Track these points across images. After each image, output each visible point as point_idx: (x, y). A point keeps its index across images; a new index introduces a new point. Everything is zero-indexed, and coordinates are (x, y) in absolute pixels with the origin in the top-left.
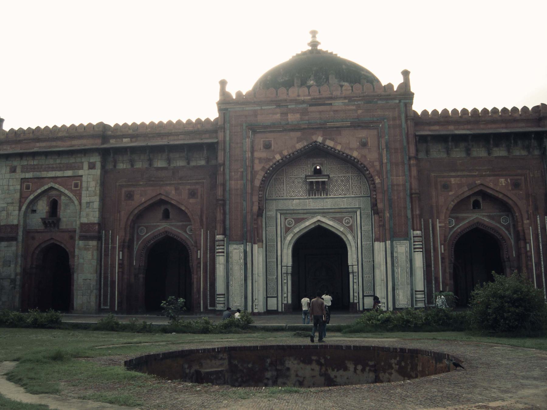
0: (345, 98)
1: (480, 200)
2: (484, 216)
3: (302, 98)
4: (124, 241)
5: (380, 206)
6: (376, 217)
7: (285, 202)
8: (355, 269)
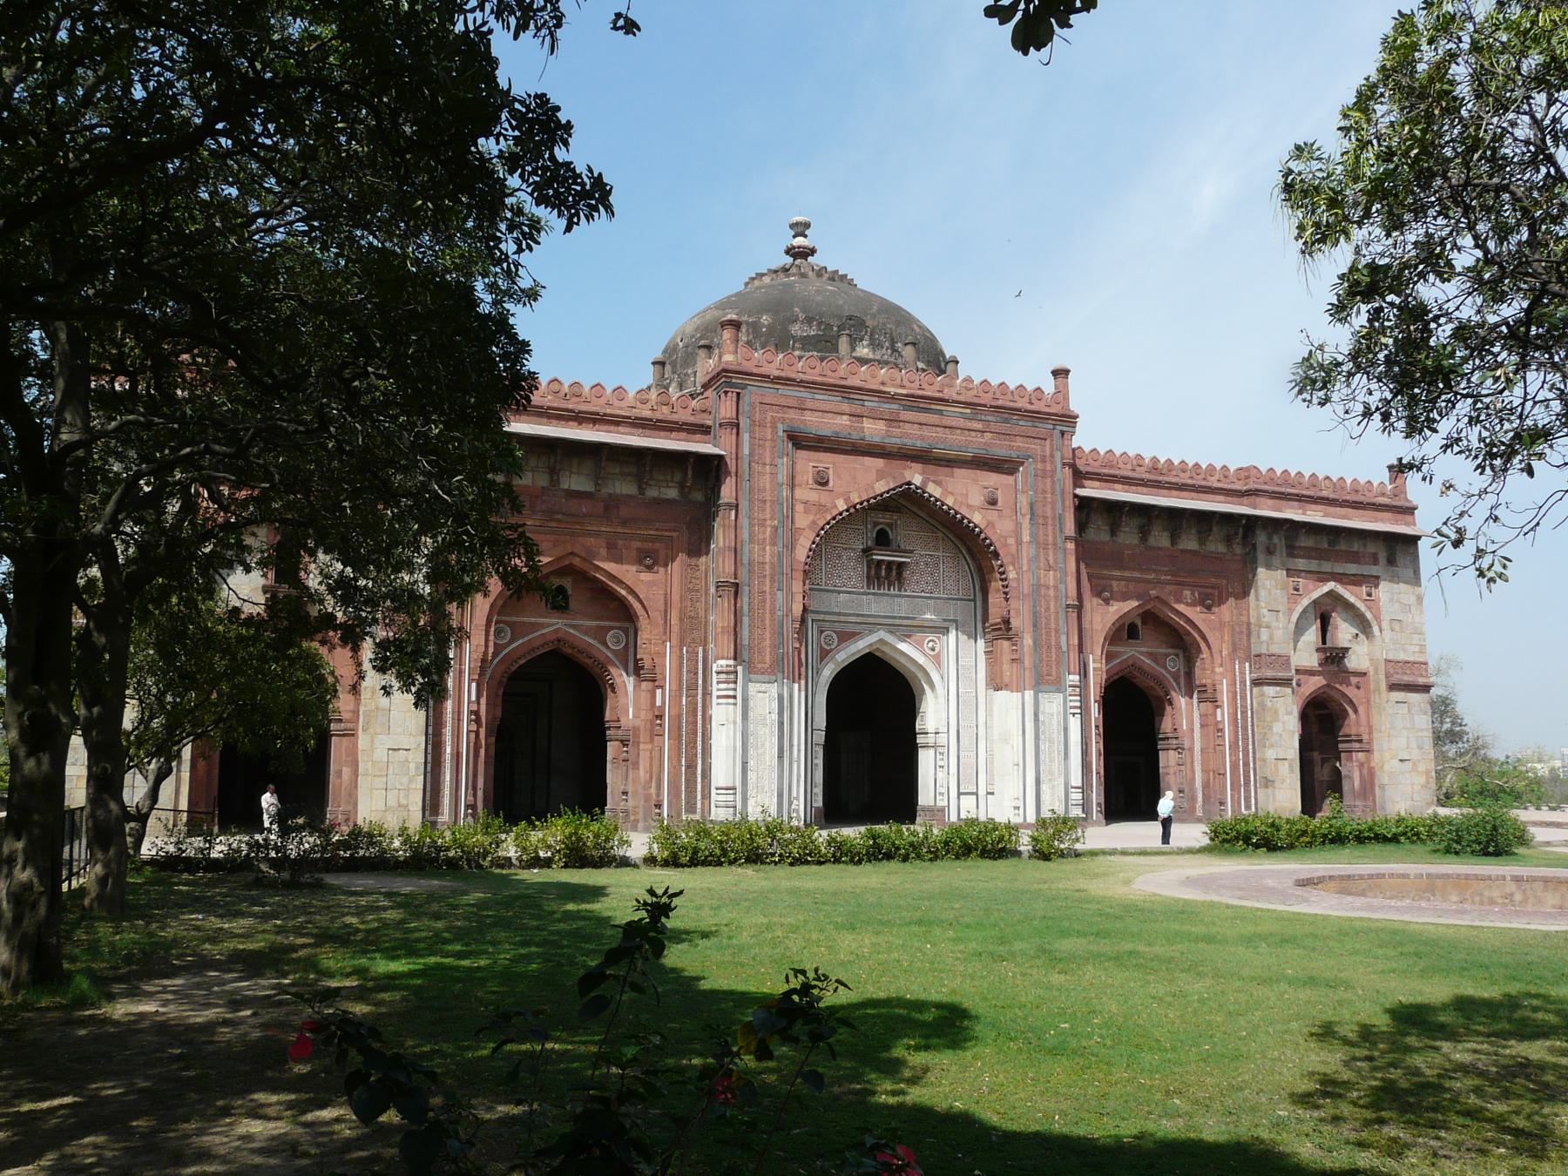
0: (967, 404)
1: (1139, 623)
2: (1142, 653)
3: (892, 390)
4: (484, 660)
5: (1014, 623)
6: (1006, 644)
7: (825, 595)
8: (942, 739)
